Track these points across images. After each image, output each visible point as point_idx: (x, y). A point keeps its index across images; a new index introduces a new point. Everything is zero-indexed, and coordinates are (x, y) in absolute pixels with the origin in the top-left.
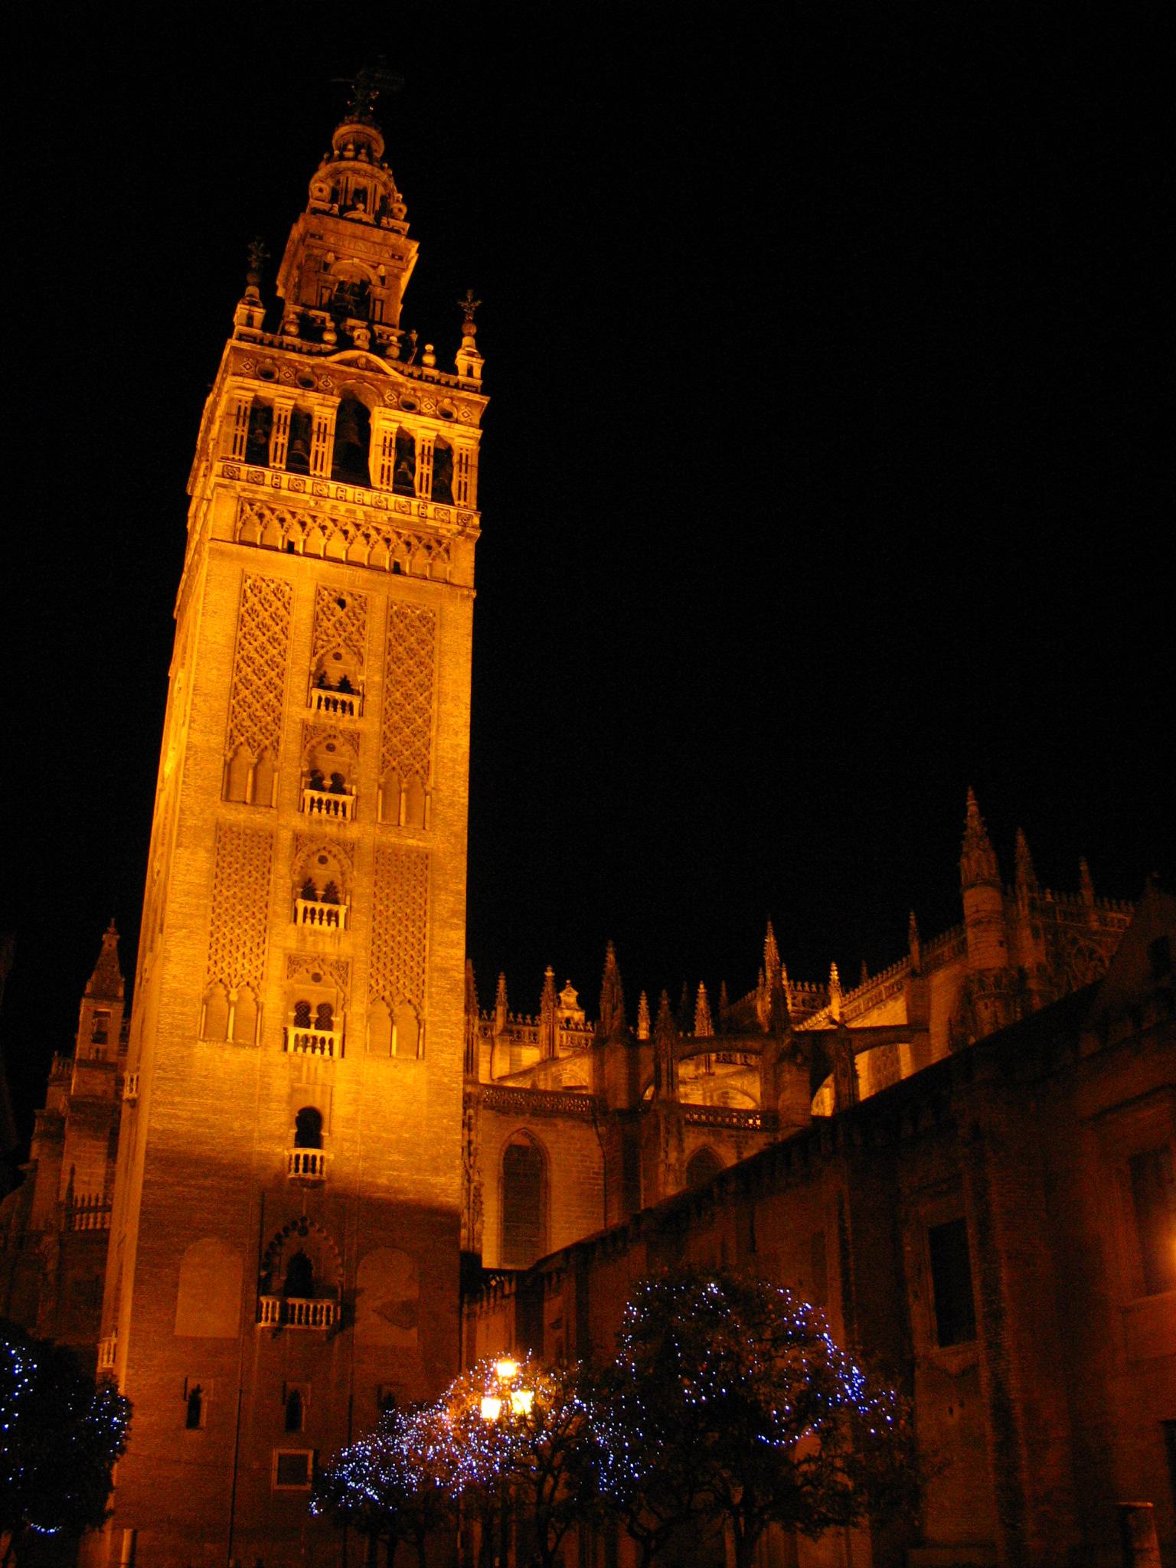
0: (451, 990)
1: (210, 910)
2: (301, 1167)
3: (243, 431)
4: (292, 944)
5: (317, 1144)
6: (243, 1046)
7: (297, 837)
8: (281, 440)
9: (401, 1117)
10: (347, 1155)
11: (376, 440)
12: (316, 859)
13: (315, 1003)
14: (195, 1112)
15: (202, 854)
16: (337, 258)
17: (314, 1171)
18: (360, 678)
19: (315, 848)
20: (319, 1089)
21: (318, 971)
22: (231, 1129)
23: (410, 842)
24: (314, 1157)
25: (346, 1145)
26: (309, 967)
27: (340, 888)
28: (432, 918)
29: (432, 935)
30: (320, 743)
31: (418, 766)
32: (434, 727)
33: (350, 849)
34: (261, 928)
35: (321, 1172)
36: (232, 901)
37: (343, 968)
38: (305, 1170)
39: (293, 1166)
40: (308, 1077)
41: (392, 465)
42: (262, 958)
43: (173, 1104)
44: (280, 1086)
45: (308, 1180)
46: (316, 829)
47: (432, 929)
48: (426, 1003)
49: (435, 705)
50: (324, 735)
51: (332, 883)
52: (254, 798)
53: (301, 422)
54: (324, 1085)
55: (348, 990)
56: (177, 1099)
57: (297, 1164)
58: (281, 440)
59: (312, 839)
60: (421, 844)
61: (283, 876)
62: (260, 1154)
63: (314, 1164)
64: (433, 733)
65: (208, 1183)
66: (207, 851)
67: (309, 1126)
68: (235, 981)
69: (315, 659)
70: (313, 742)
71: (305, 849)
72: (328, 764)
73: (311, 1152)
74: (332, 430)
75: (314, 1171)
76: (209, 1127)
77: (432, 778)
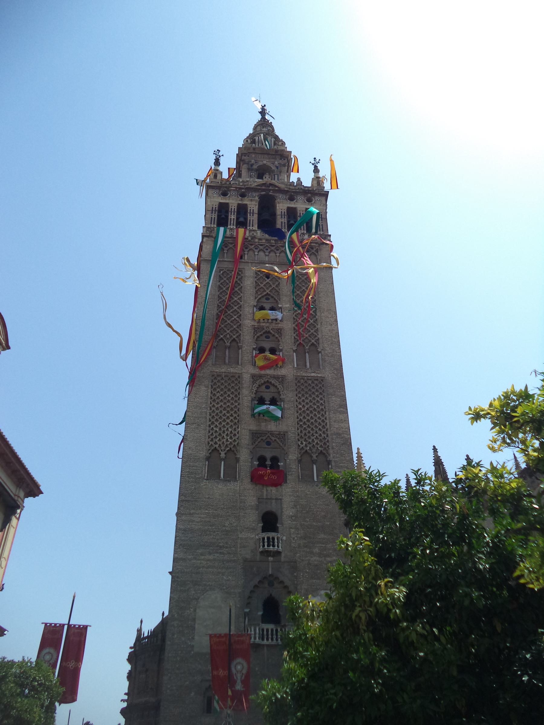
0: (343, 444)
1: (208, 414)
2: (266, 544)
3: (215, 216)
4: (253, 427)
5: (275, 529)
6: (229, 481)
7: (253, 376)
8: (232, 217)
9: (323, 514)
10: (293, 536)
11: (278, 212)
12: (264, 387)
13: (268, 455)
14: (203, 518)
15: (203, 388)
16: (256, 163)
17: (274, 546)
18: (280, 306)
19: (263, 382)
20: (274, 501)
21: (268, 440)
22: (224, 526)
23: (313, 374)
24: (273, 539)
25: (293, 530)
26: (264, 438)
27: (278, 399)
28: (329, 409)
29: (330, 418)
30: (261, 335)
31: (313, 341)
32: (319, 324)
33: (282, 379)
34: (236, 421)
35: (278, 547)
36: (220, 409)
37: (282, 436)
38: (268, 546)
39: (261, 544)
40: (267, 495)
41: (286, 221)
42: (237, 435)
43: (190, 514)
44: (252, 500)
45: (271, 551)
46: (263, 372)
47: (329, 414)
48: (331, 451)
49: (318, 314)
50: (264, 331)
51: (273, 397)
52: (229, 362)
53: (242, 210)
54: (276, 499)
55: (285, 448)
56: (192, 511)
57: (264, 543)
58: (232, 217)
59: (261, 376)
60: (319, 375)
61: (246, 395)
62: (241, 539)
63: (274, 542)
64: (319, 326)
65: (211, 557)
66: (206, 387)
67: (270, 522)
68: (223, 448)
69: (256, 300)
70: (258, 335)
71: (257, 382)
72: (267, 345)
73: (271, 535)
74: (256, 211)
75: (274, 546)
76: (211, 525)
77: (321, 345)
